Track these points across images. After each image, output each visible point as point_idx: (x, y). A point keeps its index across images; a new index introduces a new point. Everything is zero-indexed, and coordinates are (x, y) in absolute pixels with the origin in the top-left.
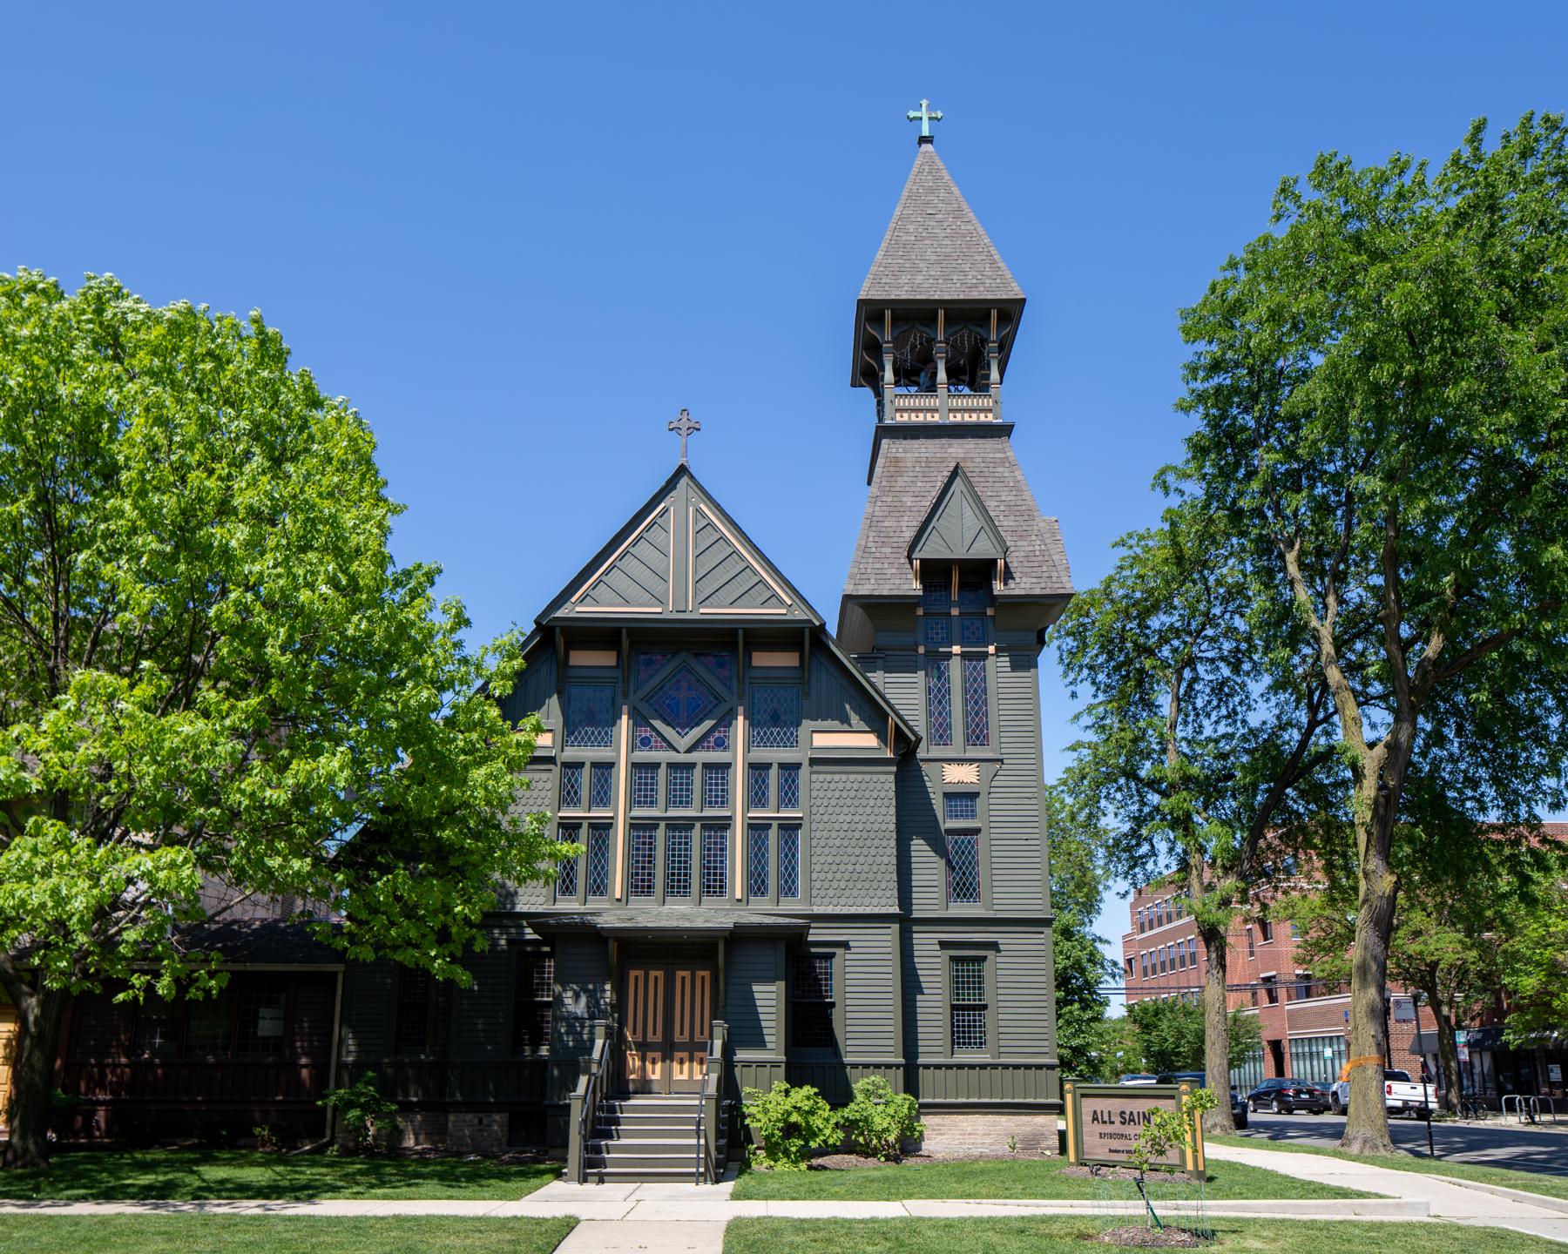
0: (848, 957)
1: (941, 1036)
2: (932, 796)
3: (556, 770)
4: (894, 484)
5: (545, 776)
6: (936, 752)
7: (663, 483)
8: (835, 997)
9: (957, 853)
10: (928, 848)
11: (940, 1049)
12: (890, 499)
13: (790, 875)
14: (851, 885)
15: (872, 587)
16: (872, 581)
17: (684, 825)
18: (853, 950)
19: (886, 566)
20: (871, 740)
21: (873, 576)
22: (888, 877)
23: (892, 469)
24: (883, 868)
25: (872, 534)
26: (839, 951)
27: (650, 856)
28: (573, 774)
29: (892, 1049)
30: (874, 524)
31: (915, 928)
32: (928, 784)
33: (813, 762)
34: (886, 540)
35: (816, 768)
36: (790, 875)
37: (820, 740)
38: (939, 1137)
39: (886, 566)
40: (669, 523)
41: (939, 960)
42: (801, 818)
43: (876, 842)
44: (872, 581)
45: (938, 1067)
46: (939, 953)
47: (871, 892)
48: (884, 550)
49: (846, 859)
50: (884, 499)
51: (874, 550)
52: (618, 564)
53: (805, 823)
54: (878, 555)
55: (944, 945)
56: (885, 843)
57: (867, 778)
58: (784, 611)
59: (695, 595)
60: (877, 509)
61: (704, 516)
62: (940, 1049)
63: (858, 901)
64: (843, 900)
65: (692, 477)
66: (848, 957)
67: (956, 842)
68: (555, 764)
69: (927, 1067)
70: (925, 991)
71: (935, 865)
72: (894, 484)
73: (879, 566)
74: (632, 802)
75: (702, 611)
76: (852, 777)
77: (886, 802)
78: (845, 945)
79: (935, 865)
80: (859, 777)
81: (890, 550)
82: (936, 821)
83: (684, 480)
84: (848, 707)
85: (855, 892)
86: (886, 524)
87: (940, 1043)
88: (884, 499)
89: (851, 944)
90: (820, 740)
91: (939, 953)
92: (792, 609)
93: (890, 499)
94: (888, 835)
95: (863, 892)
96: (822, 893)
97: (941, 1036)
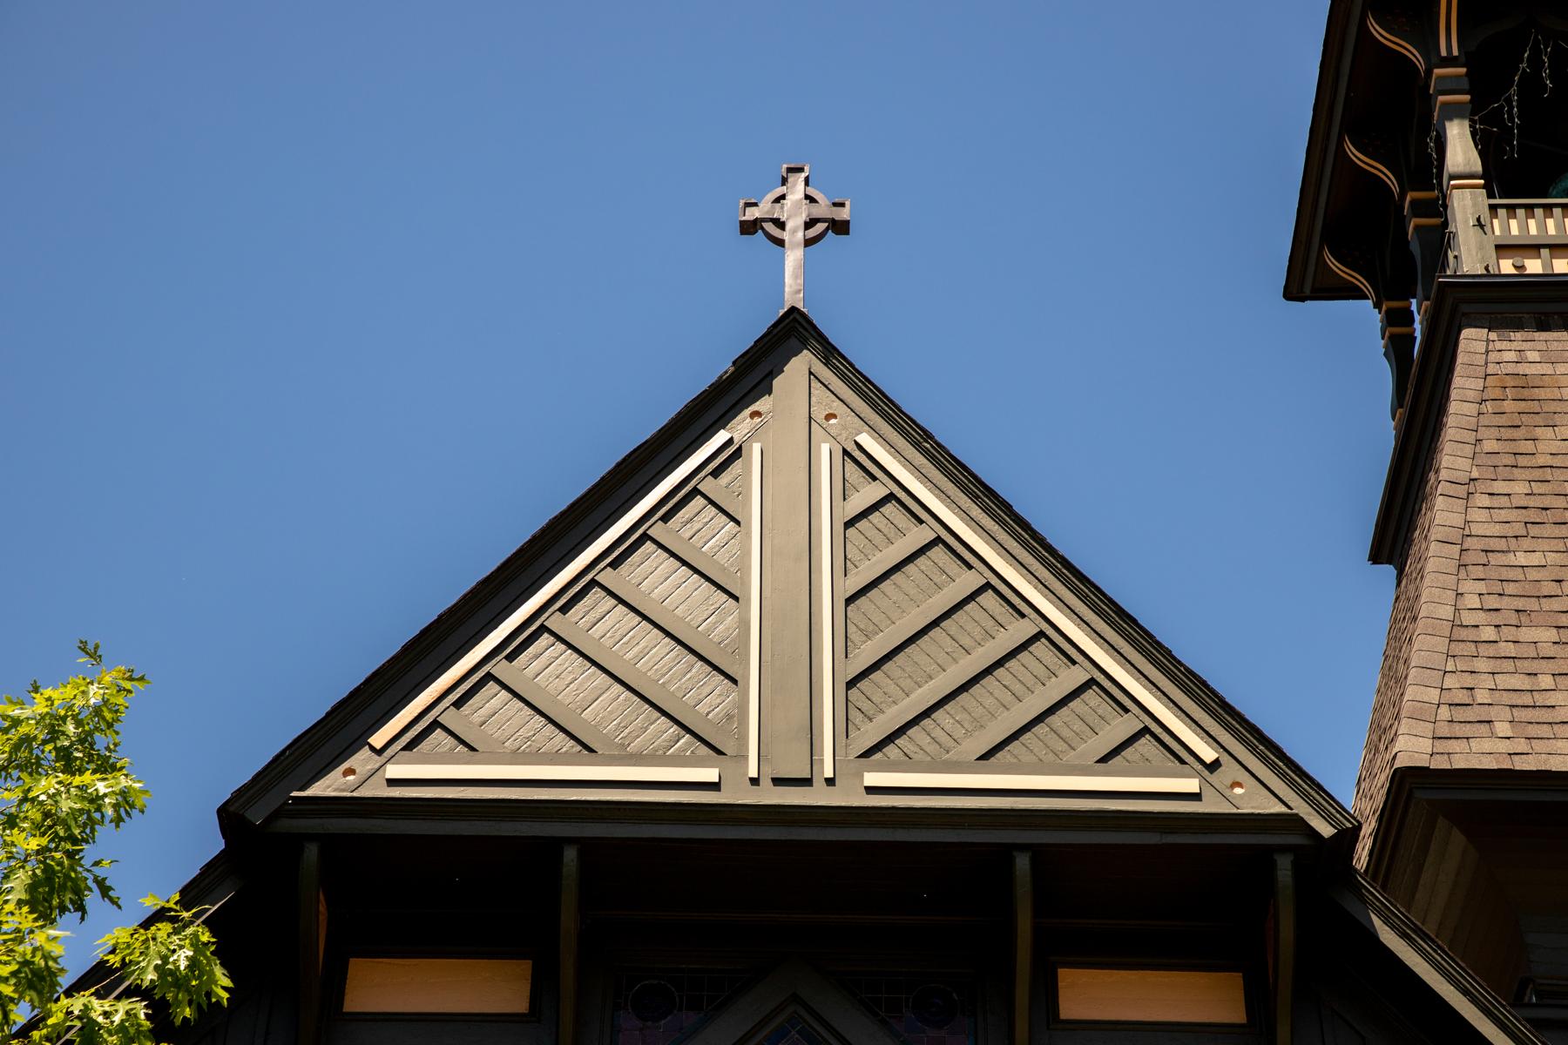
4: (1528, 447)
7: (724, 366)
12: (1520, 488)
15: (1504, 747)
16: (1503, 728)
19: (1546, 681)
21: (1501, 716)
23: (1508, 406)
25: (1468, 586)
30: (1469, 558)
34: (1532, 604)
39: (1546, 681)
40: (744, 493)
44: (1503, 728)
48: (1526, 634)
50: (1499, 487)
51: (1488, 633)
52: (554, 621)
54: (1511, 650)
58: (1191, 785)
59: (846, 727)
60: (1475, 515)
61: (871, 469)
65: (829, 353)
72: (1528, 447)
73: (1526, 683)
75: (872, 779)
81: (1552, 635)
83: (802, 363)
86: (1522, 559)
88: (1499, 487)
92: (1220, 778)
93: (1520, 488)
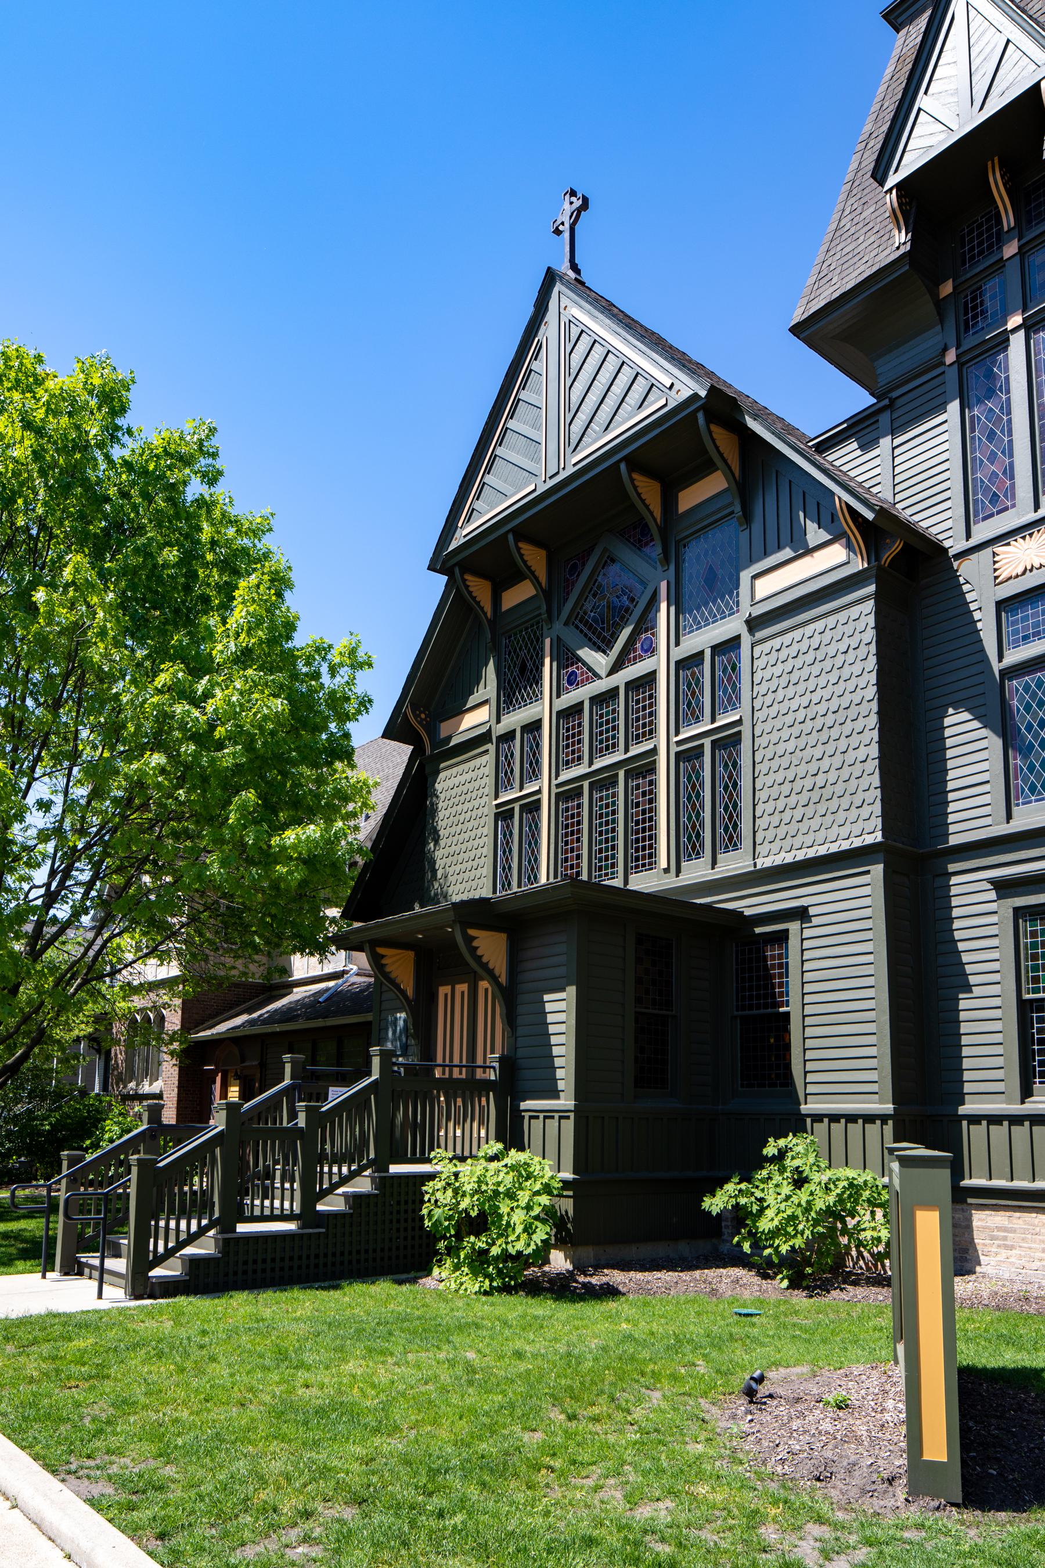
0: (807, 933)
1: (999, 1062)
2: (977, 615)
3: (491, 747)
5: (484, 759)
6: (983, 531)
8: (793, 1008)
9: (1028, 708)
10: (966, 716)
11: (1000, 1087)
13: (731, 817)
14: (810, 811)
17: (603, 781)
18: (815, 921)
20: (837, 554)
22: (864, 783)
24: (857, 771)
26: (794, 927)
27: (651, 838)
28: (509, 747)
29: (874, 1088)
31: (952, 868)
32: (969, 597)
33: (753, 624)
35: (760, 635)
36: (731, 817)
37: (766, 587)
38: (1004, 1253)
41: (994, 919)
42: (739, 722)
43: (847, 729)
45: (995, 1120)
46: (993, 907)
47: (841, 816)
49: (801, 771)
53: (746, 730)
55: (1004, 887)
56: (859, 725)
57: (831, 621)
62: (1000, 1087)
63: (820, 836)
64: (797, 842)
66: (807, 933)
67: (1027, 688)
68: (491, 741)
69: (975, 1119)
70: (973, 980)
71: (983, 744)
74: (558, 765)
76: (809, 630)
77: (863, 651)
78: (801, 914)
79: (983, 744)
80: (819, 625)
82: (986, 660)
84: (801, 514)
85: (815, 823)
87: (999, 1074)
89: (812, 911)
90: (766, 587)
91: (993, 907)
94: (864, 708)
95: (829, 818)
96: (770, 834)
97: (999, 1062)
